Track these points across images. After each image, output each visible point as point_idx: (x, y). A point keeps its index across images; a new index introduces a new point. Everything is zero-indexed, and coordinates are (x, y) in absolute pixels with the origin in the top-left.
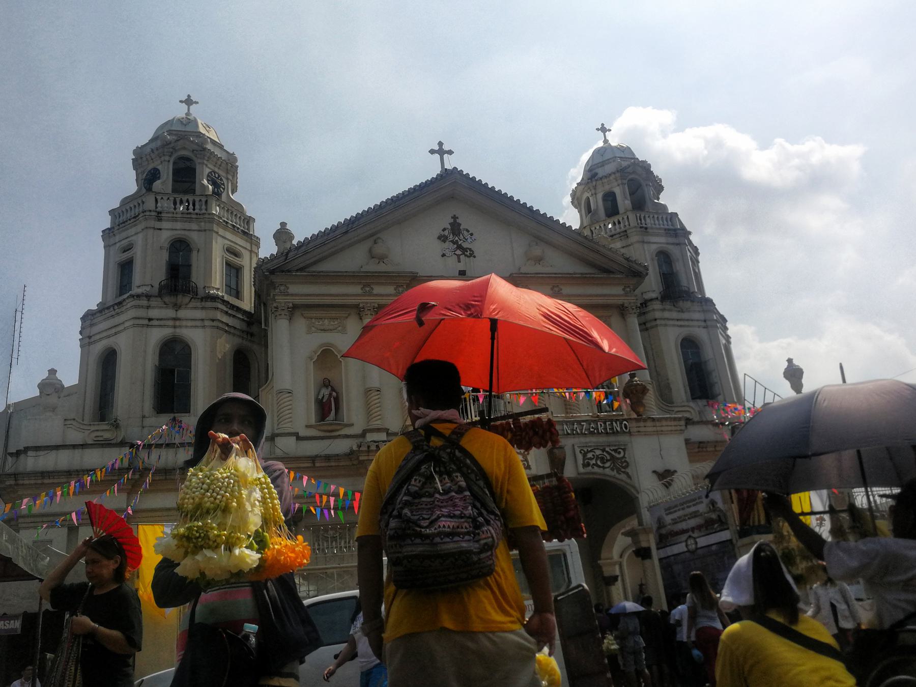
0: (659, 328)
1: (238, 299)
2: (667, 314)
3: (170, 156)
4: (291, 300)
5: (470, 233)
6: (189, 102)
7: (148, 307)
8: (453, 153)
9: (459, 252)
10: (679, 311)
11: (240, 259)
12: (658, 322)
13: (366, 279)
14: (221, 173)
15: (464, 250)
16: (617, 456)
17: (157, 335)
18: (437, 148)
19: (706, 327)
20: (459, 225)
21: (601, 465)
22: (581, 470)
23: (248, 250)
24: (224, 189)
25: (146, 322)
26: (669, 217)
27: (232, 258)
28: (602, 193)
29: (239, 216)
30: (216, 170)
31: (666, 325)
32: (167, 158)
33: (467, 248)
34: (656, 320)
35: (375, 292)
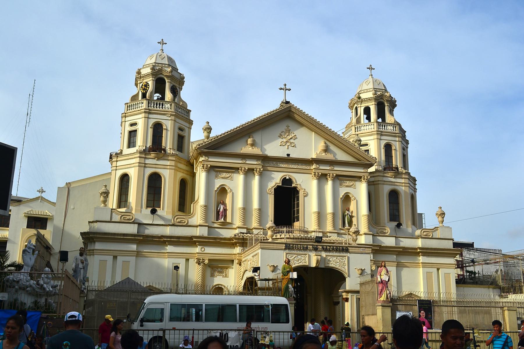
1: (182, 153)
3: (155, 78)
4: (209, 164)
5: (295, 135)
6: (162, 43)
8: (291, 90)
9: (288, 144)
11: (183, 132)
12: (380, 182)
17: (149, 171)
18: (283, 87)
20: (290, 130)
21: (335, 264)
23: (187, 127)
25: (143, 165)
26: (395, 126)
27: (181, 133)
28: (364, 107)
29: (186, 111)
30: (175, 84)
31: (384, 184)
32: (154, 79)
33: (292, 142)
34: (379, 181)
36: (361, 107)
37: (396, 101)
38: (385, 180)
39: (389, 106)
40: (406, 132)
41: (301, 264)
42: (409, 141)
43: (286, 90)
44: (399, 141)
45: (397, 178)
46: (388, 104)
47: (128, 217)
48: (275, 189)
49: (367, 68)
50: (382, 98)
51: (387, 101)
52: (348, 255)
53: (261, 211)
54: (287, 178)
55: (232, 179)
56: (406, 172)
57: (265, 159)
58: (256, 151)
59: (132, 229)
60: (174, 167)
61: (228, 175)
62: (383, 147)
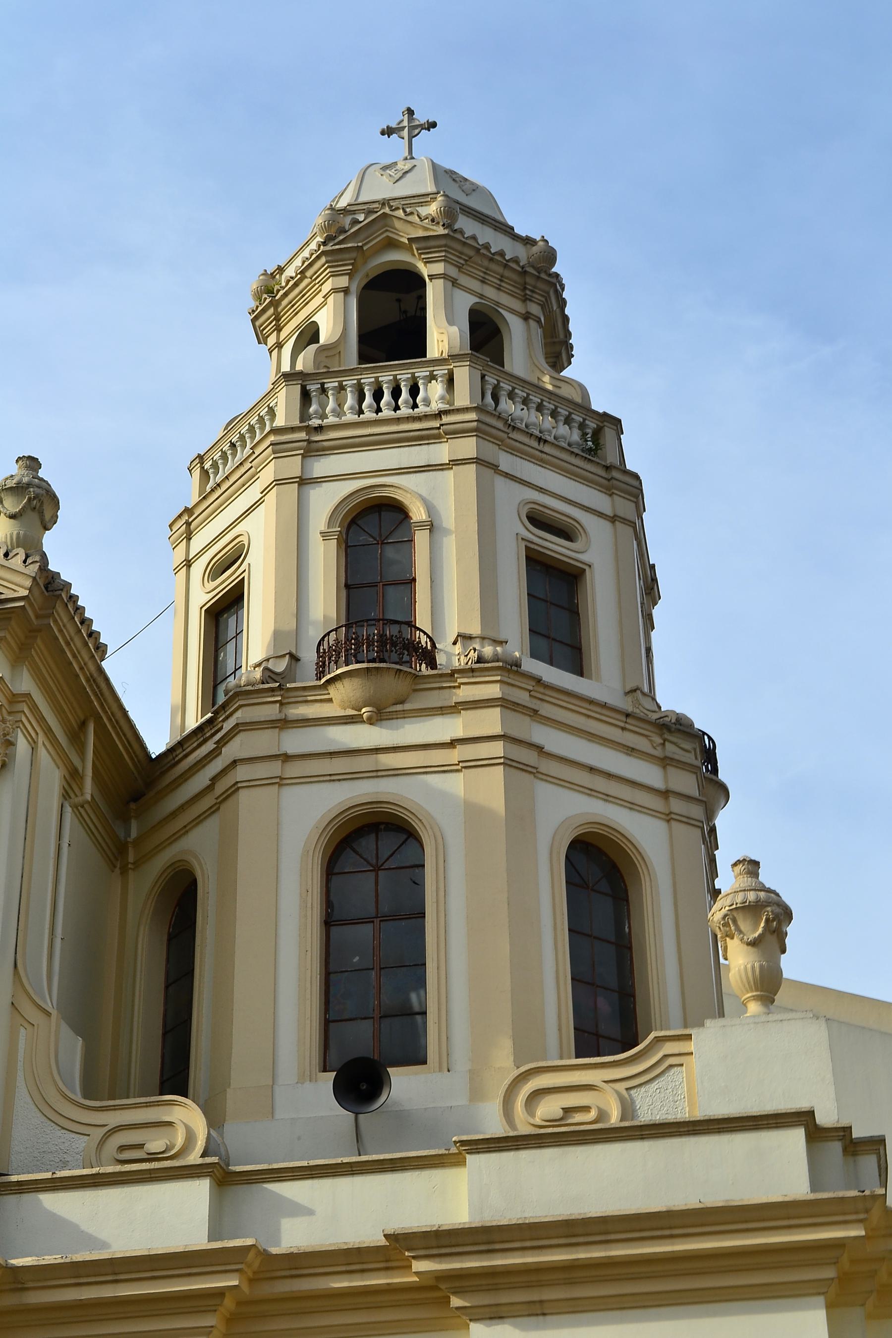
0: (244, 796)
12: (242, 773)
31: (280, 782)
34: (235, 763)
36: (279, 345)
37: (550, 256)
38: (290, 752)
39: (444, 276)
40: (616, 423)
42: (636, 477)
44: (455, 463)
45: (405, 715)
46: (439, 268)
49: (383, 133)
50: (392, 244)
51: (424, 244)
56: (480, 660)
62: (323, 527)
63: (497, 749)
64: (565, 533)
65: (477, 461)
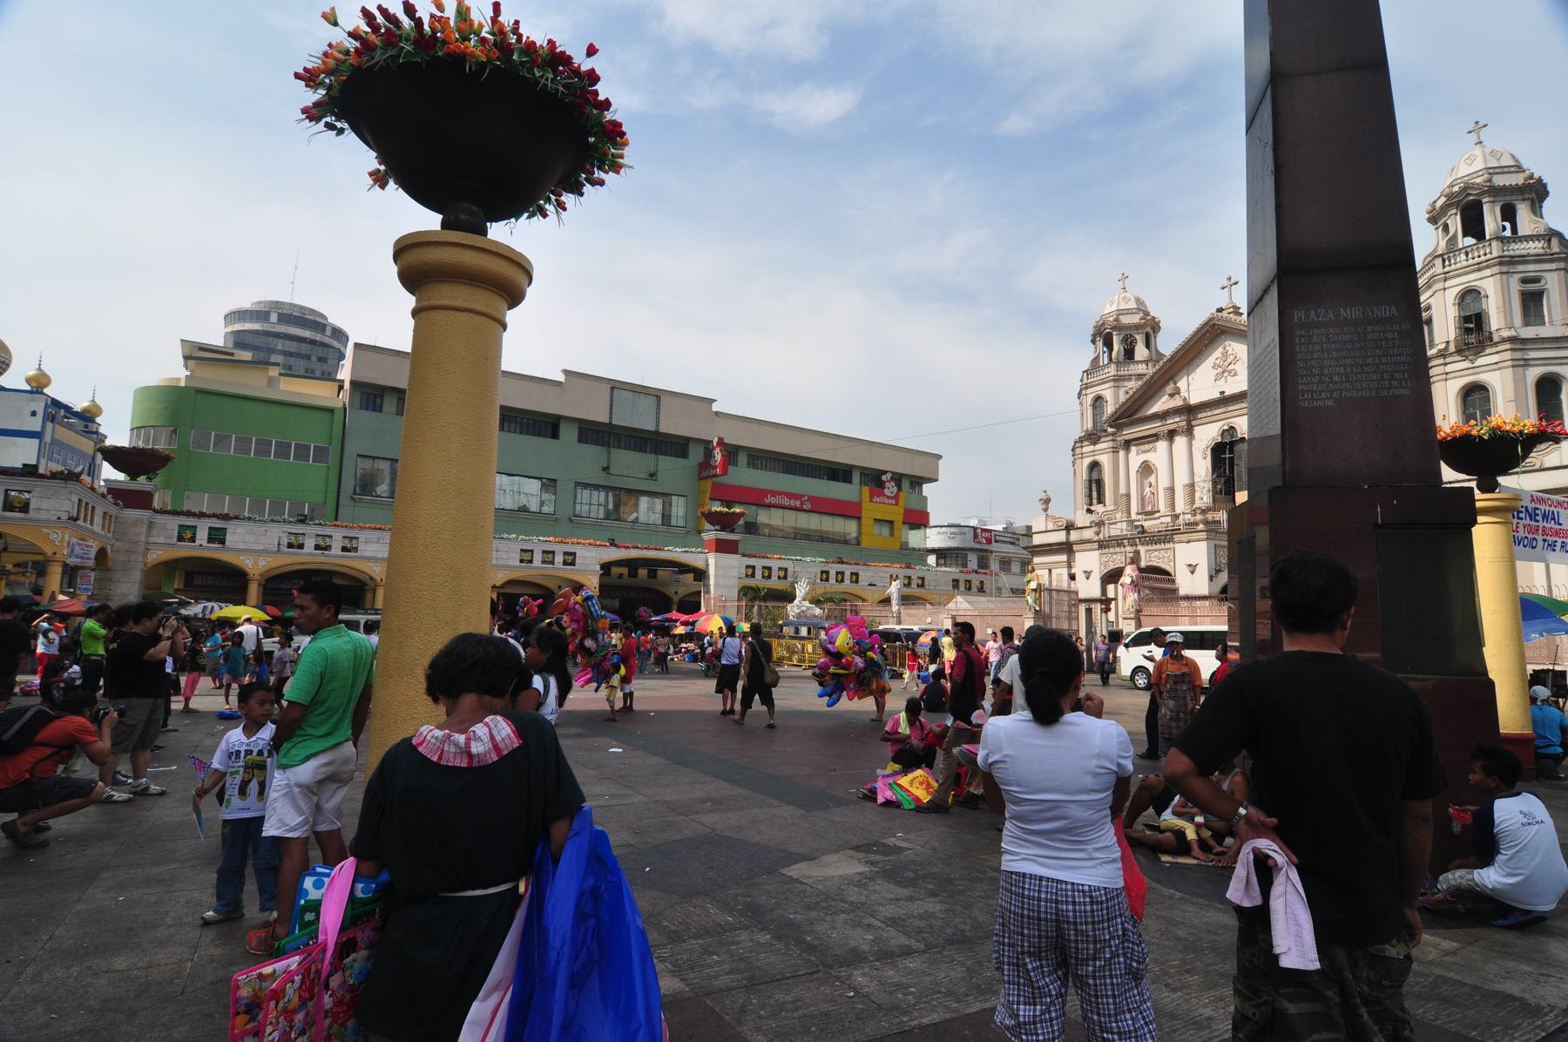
2: (1449, 368)
7: (1082, 447)
9: (1226, 374)
10: (1464, 360)
13: (1163, 416)
14: (1132, 332)
15: (1230, 372)
16: (1166, 555)
17: (1087, 461)
18: (1226, 283)
19: (1499, 369)
22: (1148, 564)
24: (1136, 343)
30: (1129, 332)
31: (1446, 380)
35: (1168, 422)
41: (1115, 567)
43: (1231, 286)
47: (1060, 524)
48: (1212, 449)
52: (1177, 546)
53: (1191, 487)
54: (1226, 427)
55: (1155, 450)
57: (1191, 412)
58: (1177, 402)
59: (1060, 537)
60: (1111, 450)
61: (1151, 446)
63: (1510, 363)
64: (1536, 280)
65: (1501, 273)
